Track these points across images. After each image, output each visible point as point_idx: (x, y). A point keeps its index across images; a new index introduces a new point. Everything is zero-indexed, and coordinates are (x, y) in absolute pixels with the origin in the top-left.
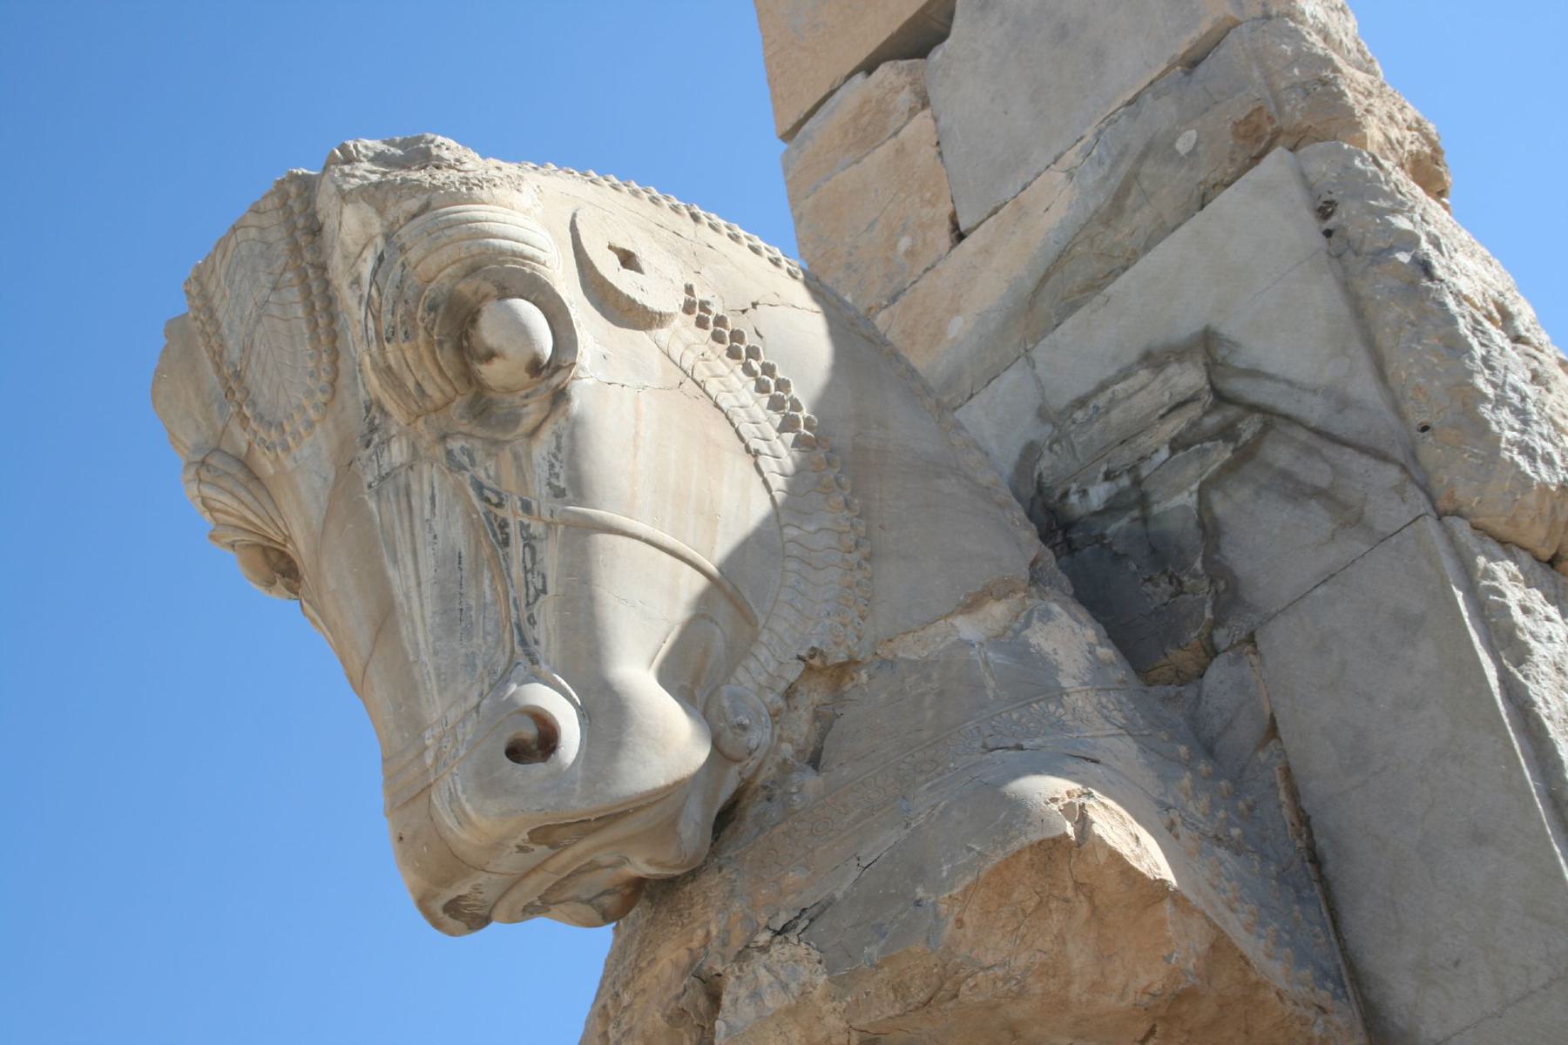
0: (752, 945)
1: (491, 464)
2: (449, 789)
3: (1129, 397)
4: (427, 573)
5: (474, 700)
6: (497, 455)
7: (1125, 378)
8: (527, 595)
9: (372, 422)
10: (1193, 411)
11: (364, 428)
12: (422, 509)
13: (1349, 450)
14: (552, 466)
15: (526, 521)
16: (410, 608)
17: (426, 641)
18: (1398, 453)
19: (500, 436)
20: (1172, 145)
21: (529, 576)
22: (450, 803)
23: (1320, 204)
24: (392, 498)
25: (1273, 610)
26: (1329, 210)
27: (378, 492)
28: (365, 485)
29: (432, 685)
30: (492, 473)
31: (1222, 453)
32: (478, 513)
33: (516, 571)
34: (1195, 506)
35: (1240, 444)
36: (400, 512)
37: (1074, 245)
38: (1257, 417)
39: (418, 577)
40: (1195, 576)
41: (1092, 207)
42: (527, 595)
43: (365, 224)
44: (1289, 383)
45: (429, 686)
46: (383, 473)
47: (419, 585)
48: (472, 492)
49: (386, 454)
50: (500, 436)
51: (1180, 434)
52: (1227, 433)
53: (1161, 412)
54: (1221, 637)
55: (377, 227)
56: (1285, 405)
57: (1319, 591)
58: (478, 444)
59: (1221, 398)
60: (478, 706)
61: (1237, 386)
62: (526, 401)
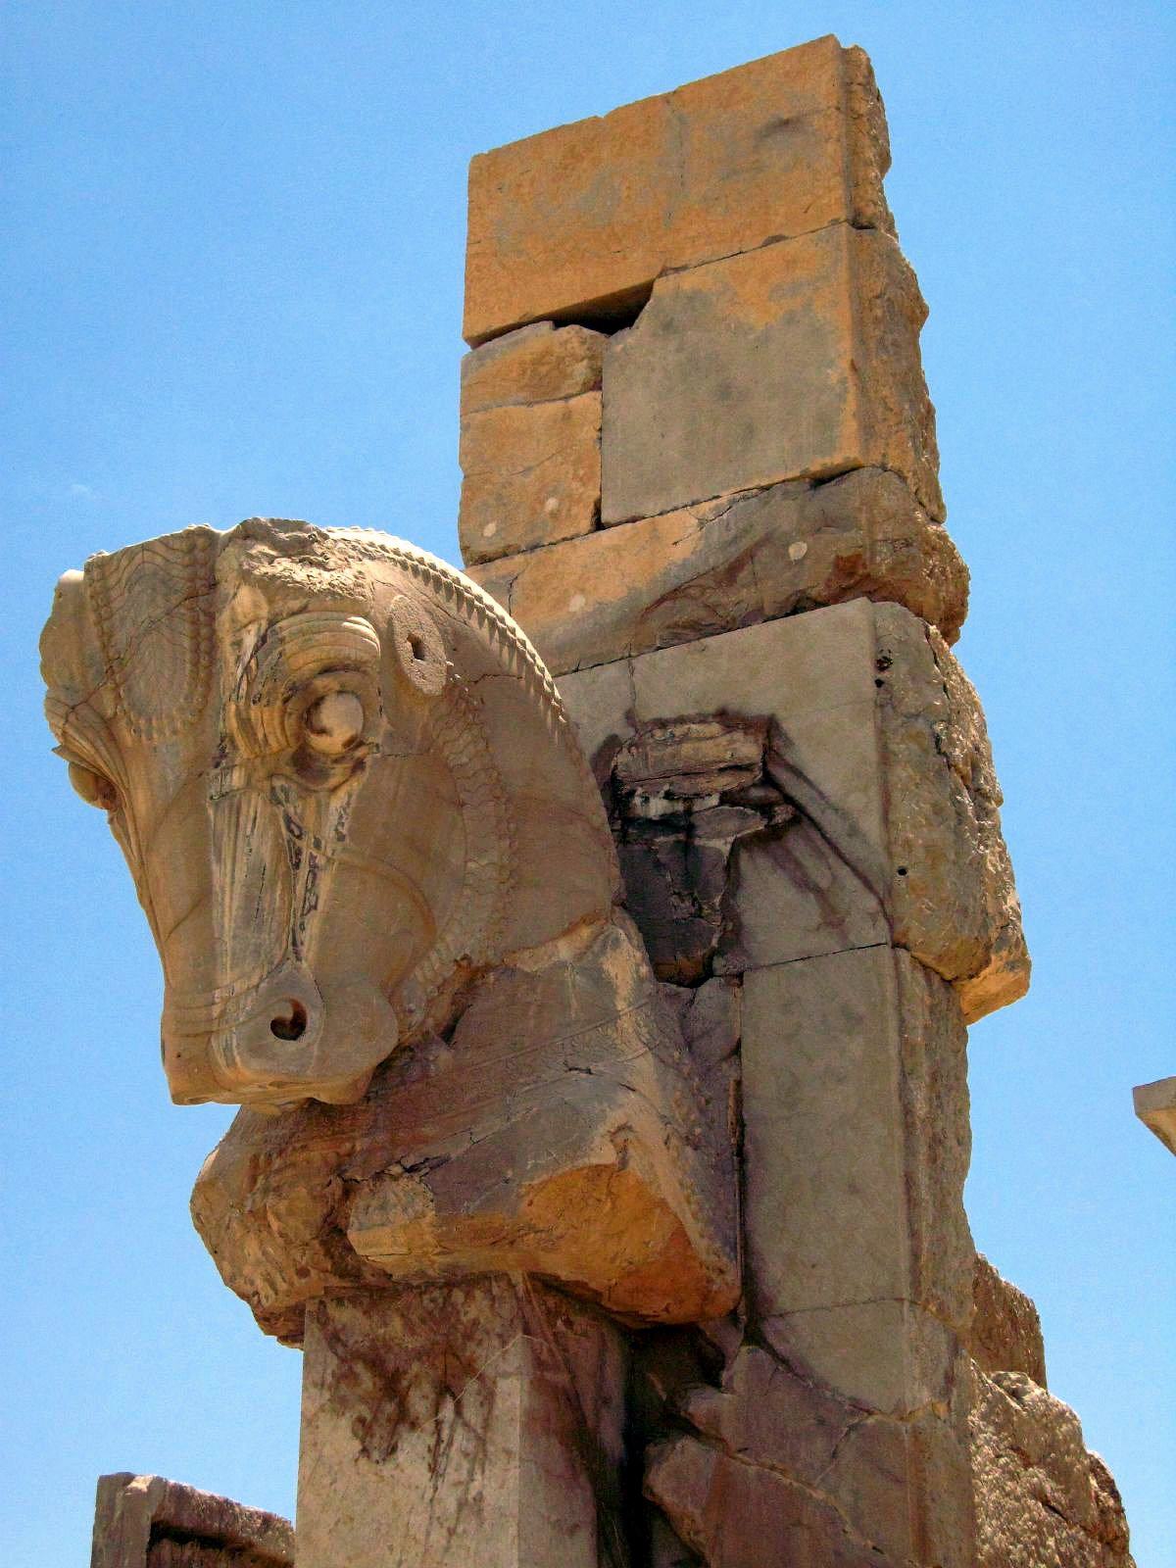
0: (386, 1172)
1: (299, 803)
2: (227, 1041)
3: (699, 739)
4: (240, 875)
5: (255, 980)
6: (305, 799)
7: (702, 722)
8: (303, 907)
9: (223, 750)
10: (746, 779)
11: (215, 752)
12: (246, 828)
13: (848, 869)
14: (341, 817)
15: (315, 854)
16: (223, 899)
17: (230, 926)
18: (880, 887)
19: (312, 787)
21: (308, 894)
22: (224, 1050)
23: (880, 657)
24: (226, 812)
25: (762, 963)
26: (886, 665)
27: (217, 804)
28: (208, 796)
29: (228, 960)
30: (299, 811)
31: (759, 825)
32: (283, 840)
33: (300, 889)
34: (727, 854)
35: (773, 823)
36: (229, 825)
37: (690, 587)
38: (790, 808)
39: (233, 877)
40: (712, 907)
42: (303, 907)
43: (256, 605)
44: (821, 794)
45: (224, 960)
46: (224, 791)
47: (233, 883)
48: (282, 823)
49: (228, 777)
50: (312, 787)
51: (730, 791)
52: (765, 809)
53: (722, 765)
54: (718, 963)
55: (264, 612)
56: (814, 810)
57: (799, 965)
58: (294, 787)
59: (768, 780)
60: (258, 986)
61: (783, 776)
62: (335, 766)
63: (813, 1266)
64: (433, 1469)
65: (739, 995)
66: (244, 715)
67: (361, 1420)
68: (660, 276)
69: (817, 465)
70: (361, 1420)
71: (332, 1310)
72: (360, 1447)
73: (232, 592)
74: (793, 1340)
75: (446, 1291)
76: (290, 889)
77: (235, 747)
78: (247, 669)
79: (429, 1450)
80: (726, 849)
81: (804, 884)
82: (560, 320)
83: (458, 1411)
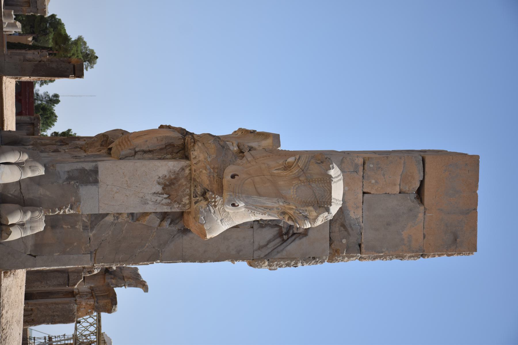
11: (287, 202)
20: (346, 239)
25: (254, 232)
33: (261, 208)
41: (347, 221)
44: (288, 246)
52: (287, 233)
56: (285, 244)
57: (252, 240)
58: (279, 211)
61: (293, 238)
63: (191, 243)
64: (154, 193)
65: (249, 227)
66: (292, 210)
67: (166, 176)
68: (425, 208)
69: (362, 246)
70: (166, 176)
71: (189, 168)
72: (160, 176)
73: (316, 211)
74: (177, 239)
75: (189, 194)
76: (260, 206)
77: (288, 205)
78: (300, 213)
79: (158, 192)
80: (280, 225)
81: (269, 242)
82: (422, 182)
83: (165, 198)
